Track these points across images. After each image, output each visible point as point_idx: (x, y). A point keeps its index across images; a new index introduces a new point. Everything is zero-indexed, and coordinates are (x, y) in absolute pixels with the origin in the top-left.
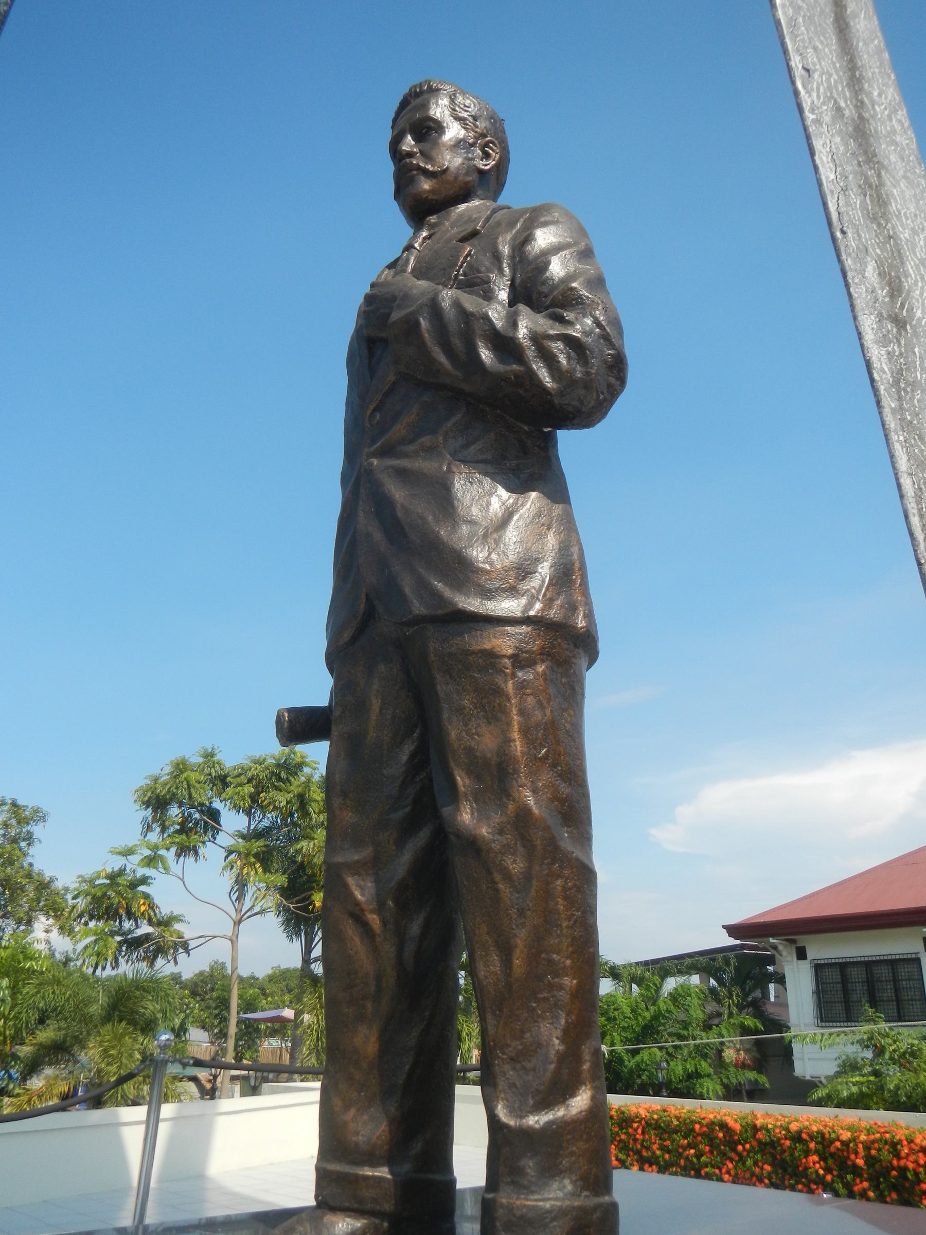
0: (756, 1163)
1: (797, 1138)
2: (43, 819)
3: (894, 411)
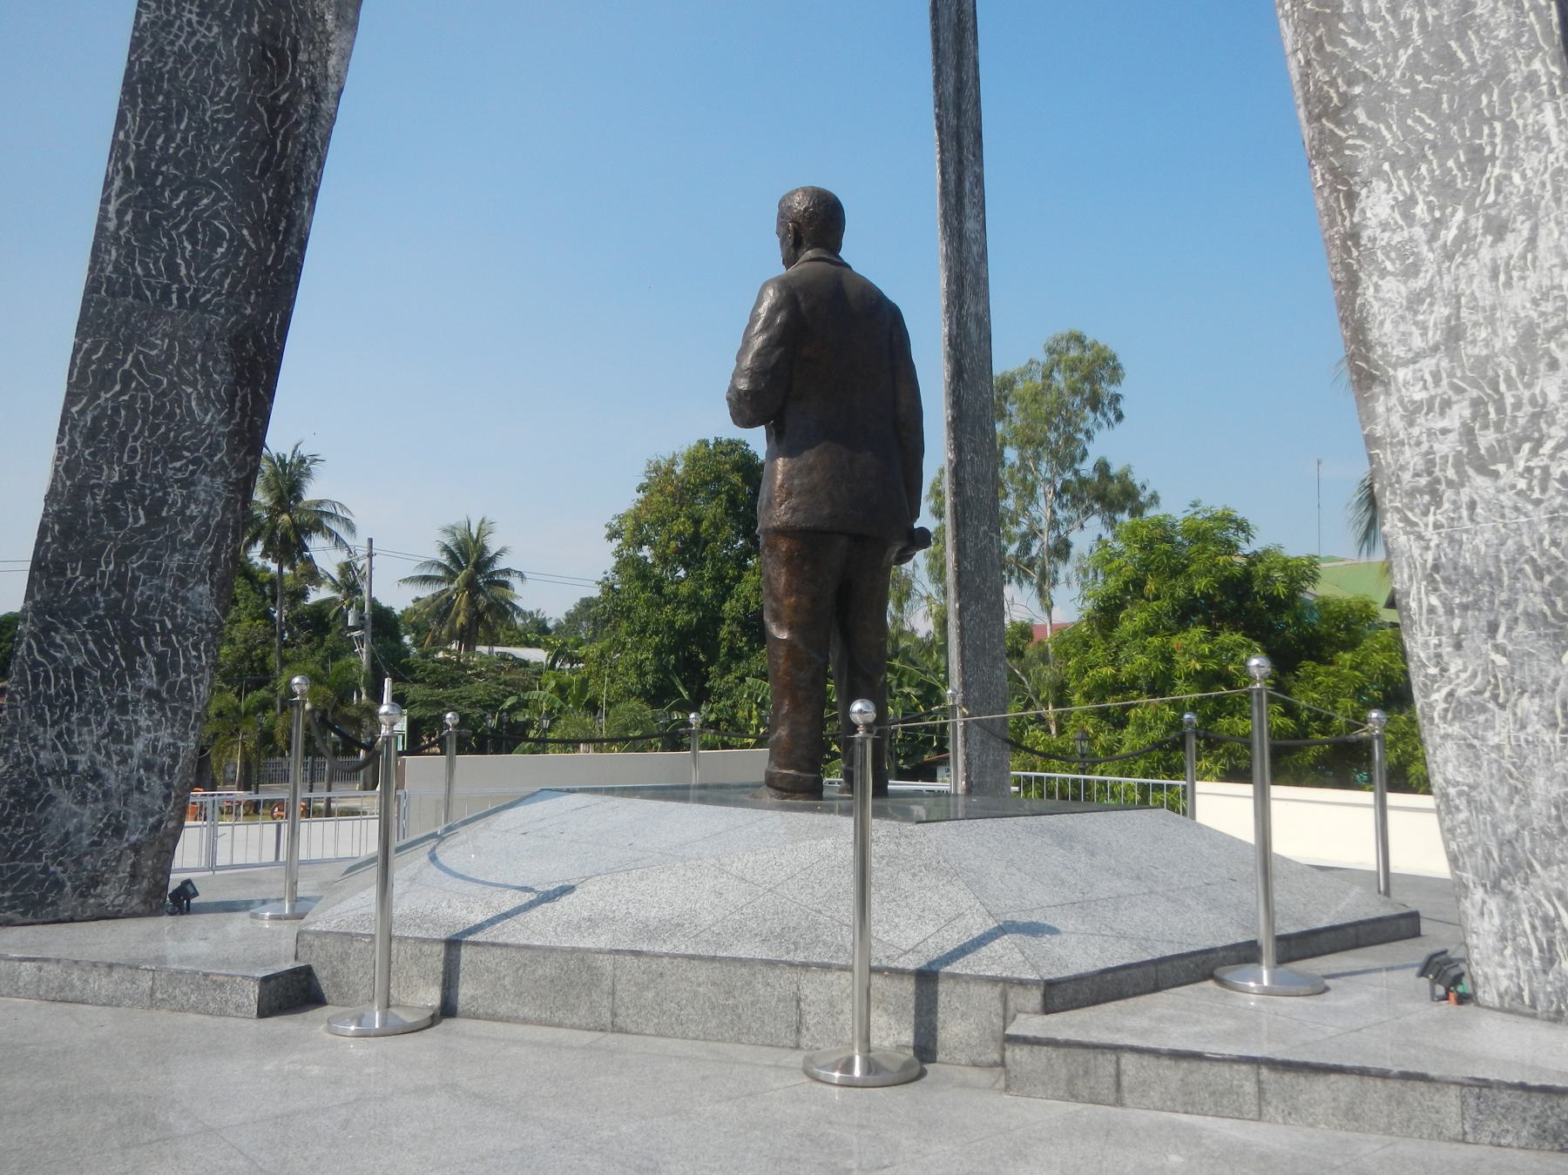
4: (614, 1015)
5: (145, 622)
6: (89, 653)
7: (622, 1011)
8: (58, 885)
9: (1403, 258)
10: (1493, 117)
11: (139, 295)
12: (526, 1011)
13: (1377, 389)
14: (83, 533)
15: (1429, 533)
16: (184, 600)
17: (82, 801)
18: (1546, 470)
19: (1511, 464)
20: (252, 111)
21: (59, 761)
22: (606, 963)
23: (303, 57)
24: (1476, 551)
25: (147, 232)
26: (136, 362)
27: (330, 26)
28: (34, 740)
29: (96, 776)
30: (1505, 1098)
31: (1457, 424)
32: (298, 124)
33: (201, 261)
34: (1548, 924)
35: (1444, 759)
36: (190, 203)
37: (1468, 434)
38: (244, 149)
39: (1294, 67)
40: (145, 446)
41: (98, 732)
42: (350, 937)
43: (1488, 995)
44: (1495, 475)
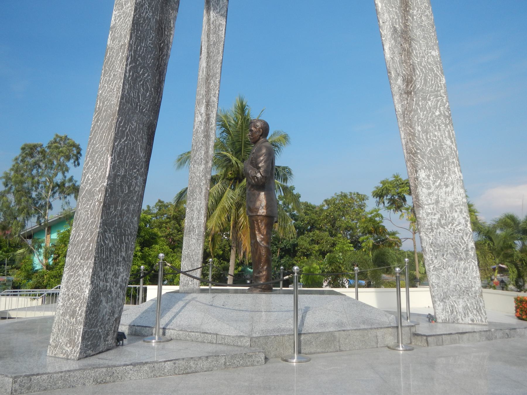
3: (401, 122)
4: (340, 347)
5: (125, 230)
6: (113, 242)
7: (341, 346)
8: (100, 337)
9: (427, 186)
10: (446, 166)
11: (131, 105)
12: (319, 350)
14: (115, 194)
15: (431, 237)
16: (132, 222)
17: (107, 303)
18: (454, 229)
19: (447, 227)
20: (156, 47)
21: (104, 285)
22: (337, 334)
23: (166, 33)
24: (440, 241)
25: (135, 80)
26: (129, 129)
27: (172, 25)
28: (99, 277)
29: (110, 292)
30: (483, 333)
32: (164, 55)
33: (144, 95)
34: (452, 306)
35: (432, 278)
36: (143, 74)
37: (439, 220)
38: (154, 59)
39: (404, 142)
40: (130, 161)
41: (112, 274)
43: (439, 320)
44: (444, 228)
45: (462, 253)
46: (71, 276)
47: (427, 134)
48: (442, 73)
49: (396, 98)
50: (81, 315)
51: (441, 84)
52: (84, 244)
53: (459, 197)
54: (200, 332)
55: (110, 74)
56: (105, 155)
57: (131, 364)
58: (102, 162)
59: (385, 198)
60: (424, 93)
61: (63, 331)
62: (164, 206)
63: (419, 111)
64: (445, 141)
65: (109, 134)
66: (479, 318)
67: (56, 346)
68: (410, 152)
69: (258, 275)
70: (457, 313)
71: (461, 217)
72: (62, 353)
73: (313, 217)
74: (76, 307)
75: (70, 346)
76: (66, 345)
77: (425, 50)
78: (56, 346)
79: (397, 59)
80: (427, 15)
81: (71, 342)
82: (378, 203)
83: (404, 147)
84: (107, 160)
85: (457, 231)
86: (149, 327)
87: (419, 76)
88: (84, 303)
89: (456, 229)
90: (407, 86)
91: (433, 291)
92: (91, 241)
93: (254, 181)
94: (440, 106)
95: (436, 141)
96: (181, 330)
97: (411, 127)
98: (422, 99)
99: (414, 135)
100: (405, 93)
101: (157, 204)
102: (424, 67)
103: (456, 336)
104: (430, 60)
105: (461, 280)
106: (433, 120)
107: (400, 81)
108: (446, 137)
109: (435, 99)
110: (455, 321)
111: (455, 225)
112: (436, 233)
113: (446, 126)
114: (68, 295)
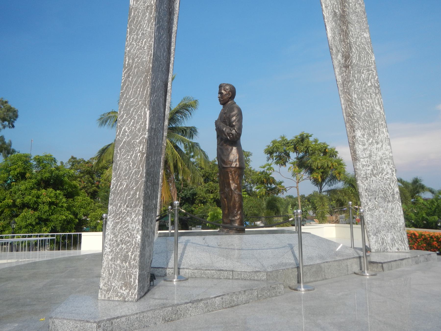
0: (422, 244)
1: (432, 237)
2: (251, 155)
3: (341, 90)
10: (376, 127)
12: (312, 280)
13: (357, 161)
15: (366, 184)
19: (378, 176)
22: (322, 265)
24: (373, 187)
30: (413, 259)
31: (370, 169)
34: (383, 239)
37: (372, 171)
39: (344, 108)
42: (277, 271)
43: (373, 250)
44: (376, 177)
45: (390, 197)
46: (118, 223)
47: (362, 101)
48: (372, 52)
49: (337, 70)
50: (134, 259)
51: (371, 60)
52: (129, 193)
53: (387, 153)
54: (216, 270)
55: (137, 32)
56: (142, 109)
57: (190, 302)
58: (140, 116)
59: (275, 154)
60: (358, 67)
61: (116, 275)
62: (77, 162)
63: (355, 81)
64: (376, 107)
65: (144, 90)
66: (403, 247)
67: (109, 290)
68: (348, 115)
69: (233, 219)
70: (386, 244)
71: (388, 168)
72: (117, 296)
73: (207, 171)
74: (127, 252)
75: (126, 289)
76: (121, 288)
77: (359, 32)
78: (109, 290)
79: (337, 38)
80: (360, 4)
81: (127, 285)
82: (268, 159)
83: (344, 111)
84: (145, 114)
85: (386, 179)
86: (162, 268)
87: (355, 53)
88: (137, 248)
89: (385, 178)
90: (346, 61)
91: (368, 228)
92: (136, 190)
93: (230, 137)
94: (371, 79)
95: (369, 107)
96: (196, 269)
97: (349, 94)
98: (358, 72)
99: (351, 102)
100: (344, 67)
101: (70, 160)
102: (359, 46)
103: (399, 262)
104: (363, 41)
105: (389, 218)
106: (366, 90)
107: (340, 57)
108: (376, 104)
109: (367, 73)
110: (385, 250)
111: (384, 174)
112: (370, 180)
113: (376, 94)
114: (116, 241)
